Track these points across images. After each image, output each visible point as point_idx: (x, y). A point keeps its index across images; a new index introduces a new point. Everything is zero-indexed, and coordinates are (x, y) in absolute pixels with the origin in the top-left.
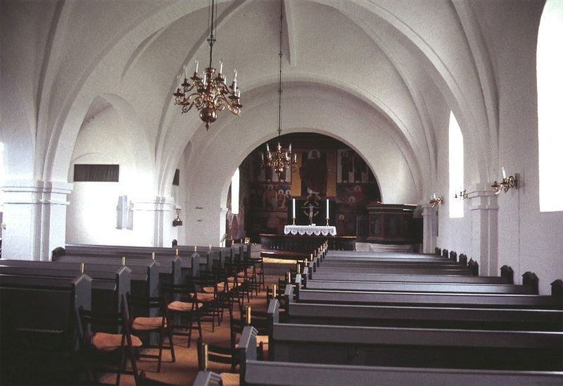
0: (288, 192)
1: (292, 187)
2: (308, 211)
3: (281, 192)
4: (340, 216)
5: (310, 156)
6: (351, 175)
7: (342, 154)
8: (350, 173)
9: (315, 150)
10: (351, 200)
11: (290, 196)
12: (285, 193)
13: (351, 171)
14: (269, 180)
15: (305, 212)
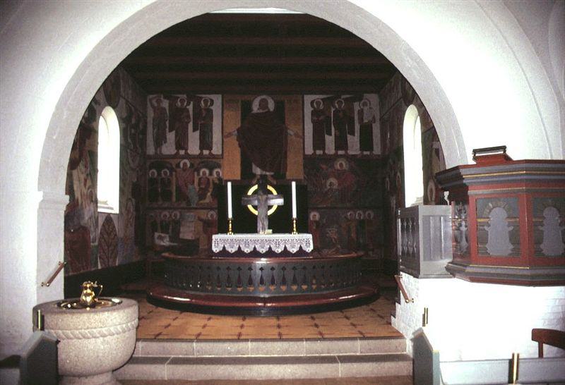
0: (218, 173)
1: (225, 162)
3: (204, 173)
5: (255, 108)
6: (330, 140)
7: (312, 103)
8: (327, 137)
9: (264, 97)
11: (220, 179)
12: (211, 174)
14: (182, 152)
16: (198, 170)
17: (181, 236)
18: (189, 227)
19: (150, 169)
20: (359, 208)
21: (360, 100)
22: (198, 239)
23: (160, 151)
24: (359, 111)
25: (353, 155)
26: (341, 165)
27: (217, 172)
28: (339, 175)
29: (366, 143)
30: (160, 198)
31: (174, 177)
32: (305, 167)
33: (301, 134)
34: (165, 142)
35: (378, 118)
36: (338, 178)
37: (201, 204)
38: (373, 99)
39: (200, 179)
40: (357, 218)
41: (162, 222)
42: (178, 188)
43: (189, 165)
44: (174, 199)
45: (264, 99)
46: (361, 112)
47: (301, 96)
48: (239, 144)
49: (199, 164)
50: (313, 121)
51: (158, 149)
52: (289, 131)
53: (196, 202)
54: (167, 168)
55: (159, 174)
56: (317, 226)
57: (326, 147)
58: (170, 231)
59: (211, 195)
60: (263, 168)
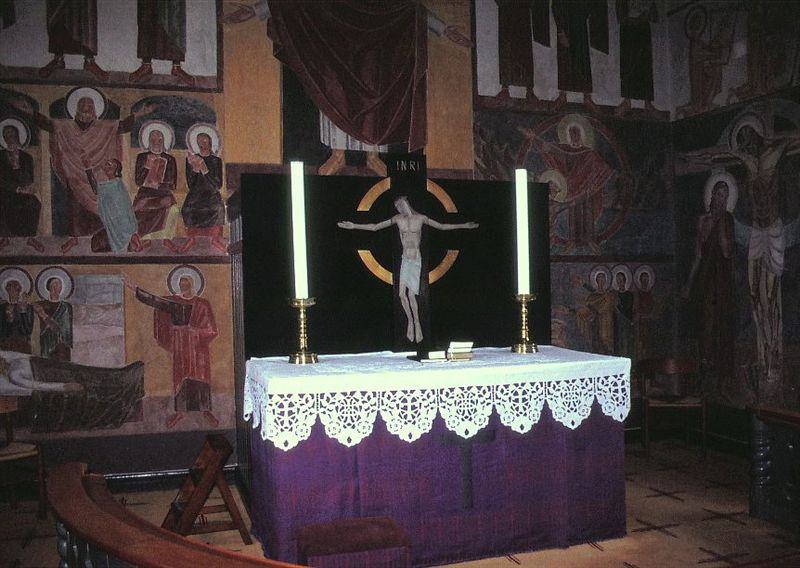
1: (227, 103)
2: (389, 250)
3: (156, 139)
6: (545, 58)
8: (536, 45)
11: (213, 162)
12: (180, 142)
14: (75, 62)
15: (365, 255)
16: (132, 127)
17: (77, 357)
20: (618, 259)
22: (139, 365)
25: (603, 107)
26: (575, 132)
27: (201, 135)
31: (45, 146)
32: (479, 132)
33: (468, 37)
37: (149, 243)
39: (142, 158)
40: (615, 286)
42: (64, 193)
43: (99, 108)
48: (276, 47)
49: (136, 106)
52: (432, 22)
53: (128, 237)
57: (536, 78)
58: (34, 341)
59: (183, 213)
60: (354, 129)
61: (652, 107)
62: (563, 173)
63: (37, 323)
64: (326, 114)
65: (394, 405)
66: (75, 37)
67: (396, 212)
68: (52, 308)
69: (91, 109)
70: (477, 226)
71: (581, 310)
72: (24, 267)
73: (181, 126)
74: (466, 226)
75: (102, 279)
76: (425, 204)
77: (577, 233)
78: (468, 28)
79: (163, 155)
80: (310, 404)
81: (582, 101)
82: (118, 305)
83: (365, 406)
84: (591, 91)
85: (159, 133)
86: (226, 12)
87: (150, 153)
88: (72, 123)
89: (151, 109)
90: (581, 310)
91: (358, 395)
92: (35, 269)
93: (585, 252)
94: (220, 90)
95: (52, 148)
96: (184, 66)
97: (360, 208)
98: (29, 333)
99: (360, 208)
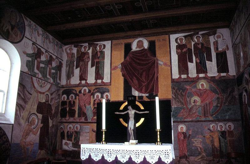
0: (107, 96)
1: (112, 88)
2: (127, 119)
4: (180, 127)
5: (134, 47)
6: (192, 67)
7: (176, 40)
8: (189, 64)
9: (141, 39)
10: (195, 101)
13: (192, 62)
14: (83, 82)
15: (121, 120)
16: (93, 94)
18: (86, 136)
19: (63, 94)
20: (219, 121)
21: (214, 33)
23: (70, 82)
24: (214, 42)
25: (212, 77)
26: (202, 85)
27: (106, 95)
28: (200, 94)
29: (222, 66)
30: (68, 115)
31: (77, 99)
32: (173, 88)
33: (170, 64)
34: (73, 76)
35: (230, 46)
36: (200, 95)
38: (225, 32)
39: (95, 101)
40: (219, 129)
41: (68, 132)
42: (80, 108)
43: (87, 91)
44: (77, 115)
45: (140, 41)
46: (216, 43)
47: (168, 36)
48: (122, 74)
49: (94, 90)
50: (177, 53)
51: (68, 81)
52: (159, 62)
53: (91, 118)
54: (74, 93)
55: (68, 98)
56: (185, 137)
58: (73, 139)
60: (140, 91)
61: (229, 75)
62: (199, 97)
63: (74, 135)
64: (133, 88)
65: (106, 152)
66: (84, 77)
67: (128, 110)
68: (76, 132)
69: (86, 91)
70: (148, 112)
71: (207, 136)
72: (72, 124)
73: (102, 94)
74: (146, 112)
75: (86, 127)
76: (136, 108)
77: (205, 114)
78: (169, 63)
79: (99, 100)
80: (88, 150)
81: (204, 76)
82: (88, 132)
83: (100, 152)
84: (207, 72)
85: (98, 95)
86: (112, 68)
87: (96, 100)
88: (82, 94)
89: (97, 90)
90: (207, 136)
91: (98, 149)
92: (74, 124)
93: (208, 119)
94: (110, 85)
95: (78, 100)
96: (104, 81)
97: (120, 109)
98: (72, 137)
99: (120, 109)
